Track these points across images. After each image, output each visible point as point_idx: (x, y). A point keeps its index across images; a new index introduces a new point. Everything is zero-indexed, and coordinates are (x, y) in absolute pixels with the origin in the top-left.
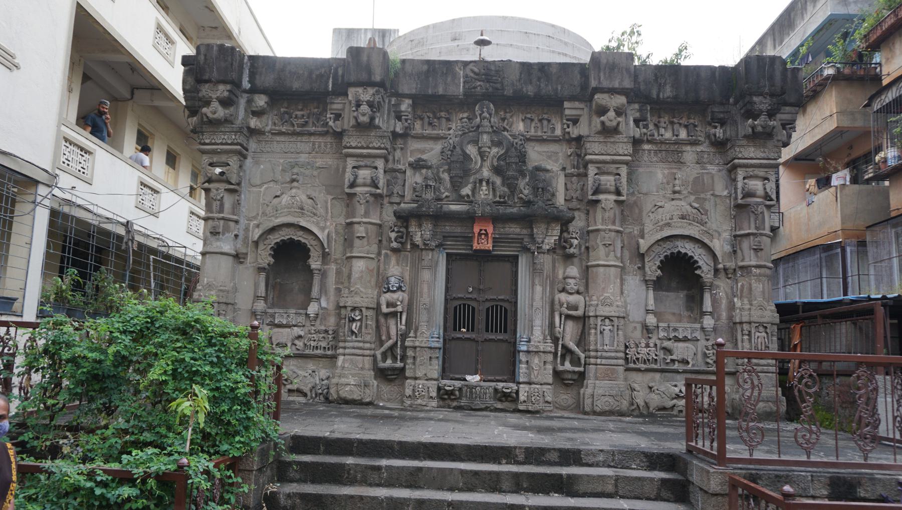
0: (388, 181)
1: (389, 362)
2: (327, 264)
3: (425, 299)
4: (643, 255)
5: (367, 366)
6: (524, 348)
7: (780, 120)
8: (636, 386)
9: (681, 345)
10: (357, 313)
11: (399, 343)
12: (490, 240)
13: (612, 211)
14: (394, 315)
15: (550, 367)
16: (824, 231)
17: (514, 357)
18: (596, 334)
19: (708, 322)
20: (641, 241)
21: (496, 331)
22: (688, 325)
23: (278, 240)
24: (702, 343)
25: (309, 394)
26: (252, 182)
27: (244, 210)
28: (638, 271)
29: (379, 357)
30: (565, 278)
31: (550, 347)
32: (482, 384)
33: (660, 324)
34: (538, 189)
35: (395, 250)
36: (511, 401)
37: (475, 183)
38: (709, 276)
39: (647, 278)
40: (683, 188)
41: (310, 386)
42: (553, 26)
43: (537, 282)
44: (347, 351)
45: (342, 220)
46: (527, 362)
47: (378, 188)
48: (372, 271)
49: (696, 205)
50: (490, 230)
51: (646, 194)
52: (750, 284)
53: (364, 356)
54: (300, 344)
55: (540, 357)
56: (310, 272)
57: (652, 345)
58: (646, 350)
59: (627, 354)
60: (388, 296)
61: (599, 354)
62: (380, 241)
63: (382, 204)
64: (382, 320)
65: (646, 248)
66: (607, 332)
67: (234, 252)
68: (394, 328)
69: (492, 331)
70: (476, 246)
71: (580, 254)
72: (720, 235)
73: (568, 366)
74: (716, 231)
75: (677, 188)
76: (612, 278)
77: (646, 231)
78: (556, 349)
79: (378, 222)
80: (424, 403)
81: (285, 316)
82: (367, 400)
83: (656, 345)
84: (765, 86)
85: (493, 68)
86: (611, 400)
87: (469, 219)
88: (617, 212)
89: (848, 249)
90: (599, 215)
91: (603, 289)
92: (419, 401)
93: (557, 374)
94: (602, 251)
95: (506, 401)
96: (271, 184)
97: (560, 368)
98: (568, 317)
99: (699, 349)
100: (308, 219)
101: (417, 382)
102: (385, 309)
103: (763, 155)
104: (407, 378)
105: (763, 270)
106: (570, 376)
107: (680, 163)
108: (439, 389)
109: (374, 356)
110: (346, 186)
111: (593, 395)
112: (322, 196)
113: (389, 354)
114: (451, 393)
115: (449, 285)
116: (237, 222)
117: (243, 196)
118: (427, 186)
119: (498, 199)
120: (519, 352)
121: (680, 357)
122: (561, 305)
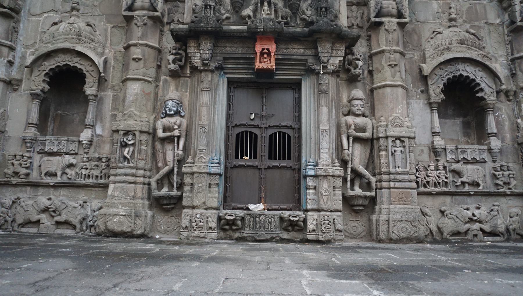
0: (169, 9)
1: (165, 191)
2: (104, 91)
3: (204, 121)
4: (426, 76)
5: (140, 195)
6: (311, 172)
8: (427, 210)
9: (470, 166)
10: (130, 137)
11: (176, 170)
12: (273, 59)
13: (396, 34)
14: (170, 140)
15: (339, 192)
17: (299, 183)
18: (387, 156)
19: (495, 143)
20: (424, 65)
21: (279, 158)
22: (476, 146)
23: (54, 67)
25: (78, 226)
26: (32, 12)
27: (22, 39)
28: (422, 94)
29: (154, 185)
30: (350, 101)
31: (339, 171)
32: (266, 212)
33: (448, 147)
34: (321, 8)
35: (174, 75)
36: (299, 230)
37: (257, 4)
38: (492, 98)
39: (432, 101)
40: (458, 17)
41: (79, 217)
43: (322, 103)
44: (118, 178)
45: (120, 48)
46: (315, 187)
47: (157, 11)
48: (149, 94)
49: (473, 31)
50: (273, 48)
51: (424, 22)
53: (136, 183)
54: (71, 172)
56: (86, 100)
57: (441, 167)
58: (435, 173)
59: (417, 177)
60: (167, 121)
61: (392, 176)
62: (159, 67)
63: (161, 31)
64: (158, 145)
65: (430, 71)
66: (398, 153)
68: (171, 154)
69: (275, 158)
70: (258, 65)
71: (364, 78)
73: (358, 191)
74: (493, 56)
75: (453, 16)
76: (400, 98)
77: (427, 56)
78: (346, 171)
79: (157, 45)
80: (202, 235)
81: (56, 143)
82: (139, 232)
83: (445, 168)
87: (252, 37)
88: (400, 34)
90: (383, 36)
92: (197, 233)
93: (347, 200)
94: (388, 72)
95: (293, 230)
96: (51, 14)
97: (351, 193)
98: (356, 139)
100: (85, 45)
101: (195, 211)
102: (160, 134)
104: (184, 207)
106: (360, 202)
108: (220, 219)
109: (149, 184)
110: (123, 9)
111: (388, 221)
112: (101, 25)
113: (166, 181)
114: (232, 223)
115: (231, 112)
116: (12, 49)
117: (21, 25)
118: (206, 6)
119: (280, 19)
120: (305, 177)
121: (470, 180)
122: (348, 127)
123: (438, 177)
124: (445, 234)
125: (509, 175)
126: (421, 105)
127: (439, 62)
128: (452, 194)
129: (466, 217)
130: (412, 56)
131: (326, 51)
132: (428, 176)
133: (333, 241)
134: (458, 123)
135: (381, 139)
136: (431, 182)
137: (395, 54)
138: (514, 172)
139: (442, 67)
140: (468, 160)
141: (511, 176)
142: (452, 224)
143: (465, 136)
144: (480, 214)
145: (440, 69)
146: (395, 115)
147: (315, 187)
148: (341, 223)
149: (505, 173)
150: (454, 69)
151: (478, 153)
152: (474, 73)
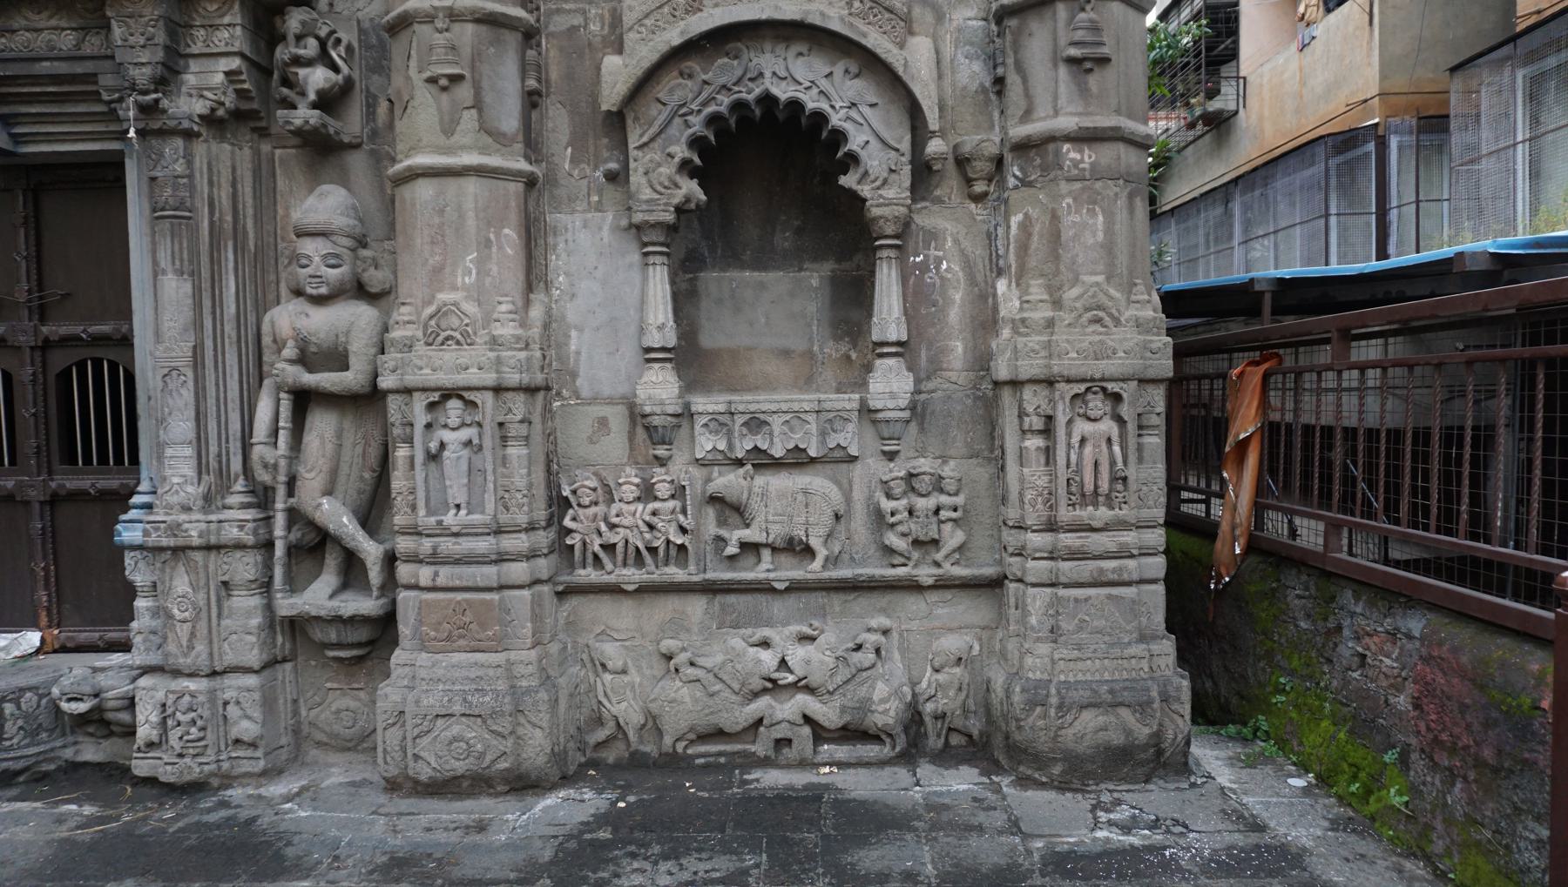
8: (611, 651)
15: (246, 603)
16: (1337, 104)
19: (890, 384)
24: (872, 468)
38: (889, 193)
39: (638, 218)
46: (154, 585)
52: (1055, 217)
55: (191, 569)
69: (88, 460)
72: (940, 17)
76: (471, 222)
77: (629, 18)
86: (472, 732)
89: (1394, 142)
91: (438, 270)
97: (287, 605)
98: (304, 401)
99: (858, 495)
105: (1109, 154)
106: (333, 637)
120: (122, 549)
121: (777, 532)
123: (651, 527)
124: (668, 740)
125: (937, 512)
126: (606, 233)
127: (664, 48)
128: (711, 589)
129: (750, 674)
130: (577, 20)
131: (142, 41)
132: (612, 527)
133: (215, 782)
134: (815, 282)
135: (391, 398)
136: (620, 548)
137: (457, 27)
138: (959, 500)
139: (693, 65)
140: (772, 457)
141: (944, 514)
142: (696, 701)
143: (837, 338)
144: (808, 662)
145: (681, 74)
146: (443, 297)
147: (154, 585)
148: (257, 714)
149: (921, 504)
150: (739, 73)
151: (813, 428)
152: (824, 84)
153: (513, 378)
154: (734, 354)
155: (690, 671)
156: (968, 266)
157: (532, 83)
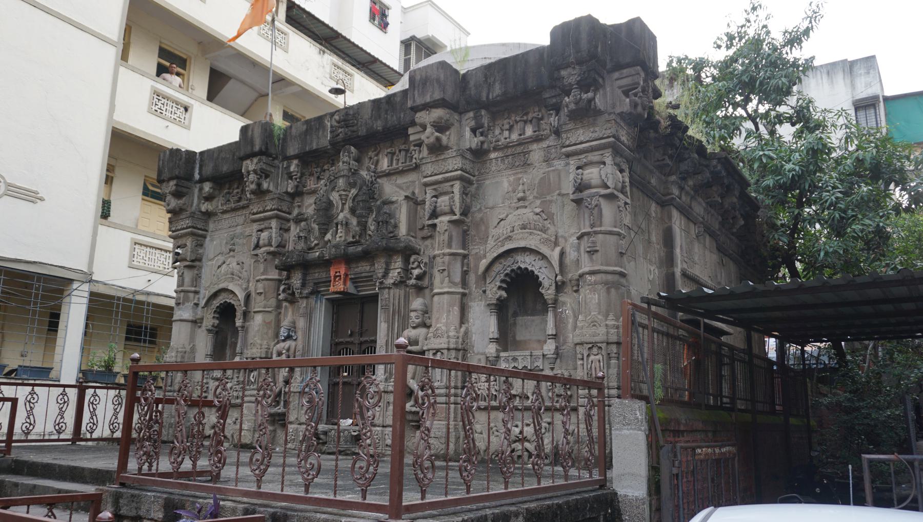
7: (620, 87)
13: (447, 233)
42: (503, 45)
48: (270, 323)
51: (492, 208)
67: (191, 318)
75: (521, 195)
84: (570, 55)
85: (351, 113)
88: (454, 234)
103: (595, 135)
105: (598, 277)
107: (526, 165)
153: (452, 346)
154: (525, 342)
155: (496, 433)
156: (574, 311)
157: (465, 268)
